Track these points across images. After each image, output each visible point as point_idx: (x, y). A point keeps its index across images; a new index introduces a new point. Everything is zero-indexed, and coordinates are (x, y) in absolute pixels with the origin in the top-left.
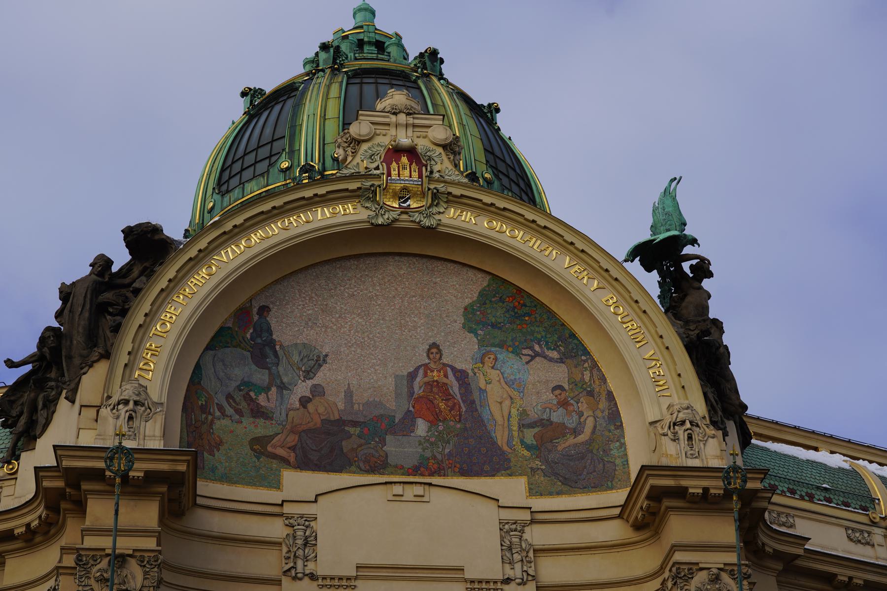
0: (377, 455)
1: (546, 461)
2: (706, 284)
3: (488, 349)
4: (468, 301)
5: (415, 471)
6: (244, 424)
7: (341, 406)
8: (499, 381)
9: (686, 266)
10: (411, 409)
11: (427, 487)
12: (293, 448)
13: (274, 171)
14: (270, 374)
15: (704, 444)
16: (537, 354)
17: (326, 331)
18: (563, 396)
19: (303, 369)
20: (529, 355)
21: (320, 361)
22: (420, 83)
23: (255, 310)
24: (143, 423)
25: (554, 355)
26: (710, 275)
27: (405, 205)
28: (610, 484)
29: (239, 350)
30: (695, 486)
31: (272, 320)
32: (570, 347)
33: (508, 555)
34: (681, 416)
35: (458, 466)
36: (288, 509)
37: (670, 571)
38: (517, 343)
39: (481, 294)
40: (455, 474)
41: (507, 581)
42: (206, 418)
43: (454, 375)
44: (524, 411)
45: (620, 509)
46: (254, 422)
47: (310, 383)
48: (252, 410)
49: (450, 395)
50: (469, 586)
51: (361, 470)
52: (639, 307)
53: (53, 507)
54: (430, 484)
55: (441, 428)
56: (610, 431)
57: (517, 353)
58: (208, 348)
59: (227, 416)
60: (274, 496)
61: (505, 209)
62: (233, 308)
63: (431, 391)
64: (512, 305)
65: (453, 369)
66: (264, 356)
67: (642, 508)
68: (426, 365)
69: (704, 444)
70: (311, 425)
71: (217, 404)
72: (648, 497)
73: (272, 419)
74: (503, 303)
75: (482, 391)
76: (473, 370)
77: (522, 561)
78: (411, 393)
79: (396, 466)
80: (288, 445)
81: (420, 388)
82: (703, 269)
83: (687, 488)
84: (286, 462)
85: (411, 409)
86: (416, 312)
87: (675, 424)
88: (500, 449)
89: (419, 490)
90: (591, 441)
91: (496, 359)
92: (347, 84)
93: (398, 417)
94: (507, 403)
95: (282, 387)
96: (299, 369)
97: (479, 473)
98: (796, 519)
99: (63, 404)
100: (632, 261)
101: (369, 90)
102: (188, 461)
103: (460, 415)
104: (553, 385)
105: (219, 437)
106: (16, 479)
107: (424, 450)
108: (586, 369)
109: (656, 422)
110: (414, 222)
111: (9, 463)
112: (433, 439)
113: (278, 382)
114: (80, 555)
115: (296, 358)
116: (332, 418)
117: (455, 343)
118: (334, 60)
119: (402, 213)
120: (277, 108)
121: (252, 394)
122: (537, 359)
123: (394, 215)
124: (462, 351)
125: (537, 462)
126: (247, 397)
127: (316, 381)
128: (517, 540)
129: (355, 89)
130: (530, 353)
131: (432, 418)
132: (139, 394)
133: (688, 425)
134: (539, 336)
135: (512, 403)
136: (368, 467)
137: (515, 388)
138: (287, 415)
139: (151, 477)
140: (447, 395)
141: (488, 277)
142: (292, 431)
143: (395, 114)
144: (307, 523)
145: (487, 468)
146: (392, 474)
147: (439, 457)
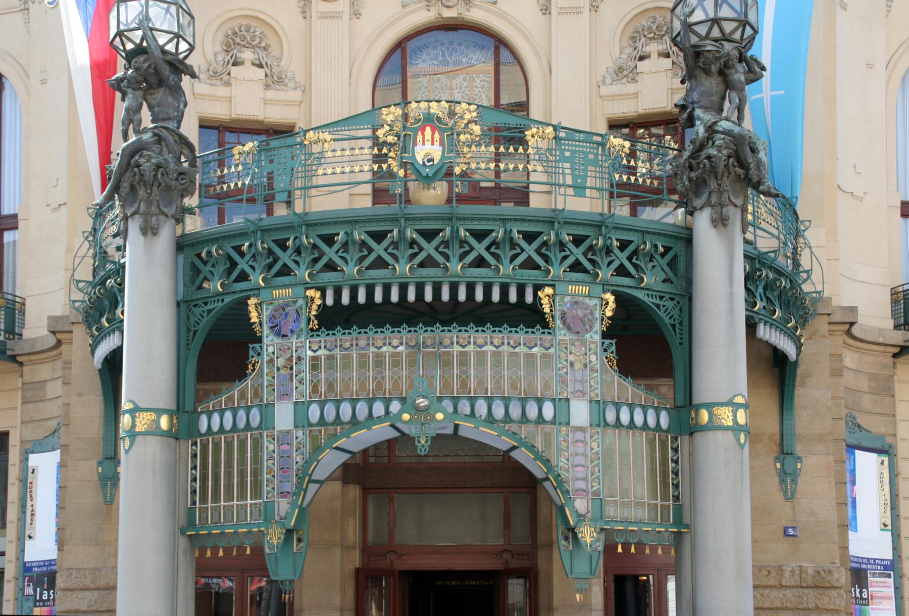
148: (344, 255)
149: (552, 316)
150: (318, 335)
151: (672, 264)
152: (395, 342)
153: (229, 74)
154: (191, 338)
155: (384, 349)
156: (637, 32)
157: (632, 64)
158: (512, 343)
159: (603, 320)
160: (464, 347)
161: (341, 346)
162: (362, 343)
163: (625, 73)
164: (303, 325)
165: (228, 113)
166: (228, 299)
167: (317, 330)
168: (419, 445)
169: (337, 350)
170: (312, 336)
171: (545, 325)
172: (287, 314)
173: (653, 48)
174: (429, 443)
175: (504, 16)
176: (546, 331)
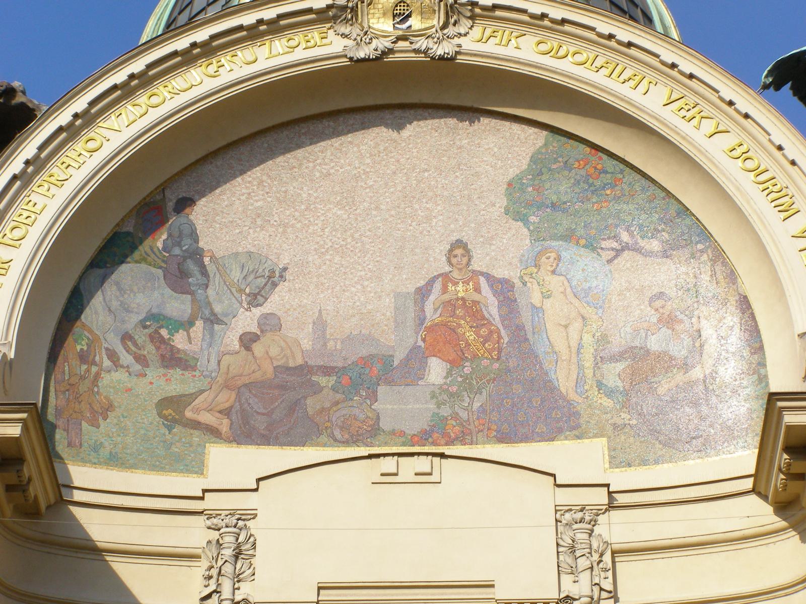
4: (512, 172)
6: (149, 378)
7: (306, 344)
8: (564, 293)
11: (436, 460)
12: (226, 412)
14: (194, 301)
16: (625, 247)
17: (284, 232)
19: (247, 291)
20: (613, 249)
21: (274, 278)
23: (171, 205)
25: (655, 245)
29: (143, 266)
33: (570, 560)
36: (212, 502)
39: (534, 159)
40: (488, 440)
42: (88, 371)
45: (752, 479)
46: (165, 375)
47: (257, 312)
48: (163, 357)
49: (484, 318)
51: (336, 440)
52: (784, 155)
54: (442, 456)
55: (467, 370)
57: (592, 246)
59: (122, 366)
60: (191, 485)
61: (564, 21)
62: (135, 199)
63: (453, 315)
65: (488, 277)
66: (184, 274)
68: (446, 277)
70: (258, 375)
71: (107, 349)
73: (194, 368)
75: (537, 310)
76: (521, 277)
77: (592, 568)
78: (421, 320)
79: (393, 433)
80: (218, 408)
81: (436, 310)
84: (214, 433)
85: (420, 343)
86: (430, 194)
88: (564, 398)
89: (423, 464)
91: (559, 258)
93: (399, 356)
95: (213, 320)
96: (241, 291)
97: (526, 439)
100: (777, 88)
103: (500, 351)
104: (649, 294)
105: (106, 398)
107: (439, 407)
110: (416, 51)
112: (455, 389)
113: (207, 312)
115: (236, 275)
116: (291, 364)
117: (492, 238)
119: (399, 39)
121: (164, 332)
123: (385, 43)
124: (503, 249)
125: (623, 415)
126: (157, 339)
127: (267, 308)
128: (586, 536)
130: (615, 245)
136: (347, 436)
138: (219, 362)
141: (545, 133)
142: (227, 386)
144: (241, 523)
146: (386, 444)
147: (464, 415)
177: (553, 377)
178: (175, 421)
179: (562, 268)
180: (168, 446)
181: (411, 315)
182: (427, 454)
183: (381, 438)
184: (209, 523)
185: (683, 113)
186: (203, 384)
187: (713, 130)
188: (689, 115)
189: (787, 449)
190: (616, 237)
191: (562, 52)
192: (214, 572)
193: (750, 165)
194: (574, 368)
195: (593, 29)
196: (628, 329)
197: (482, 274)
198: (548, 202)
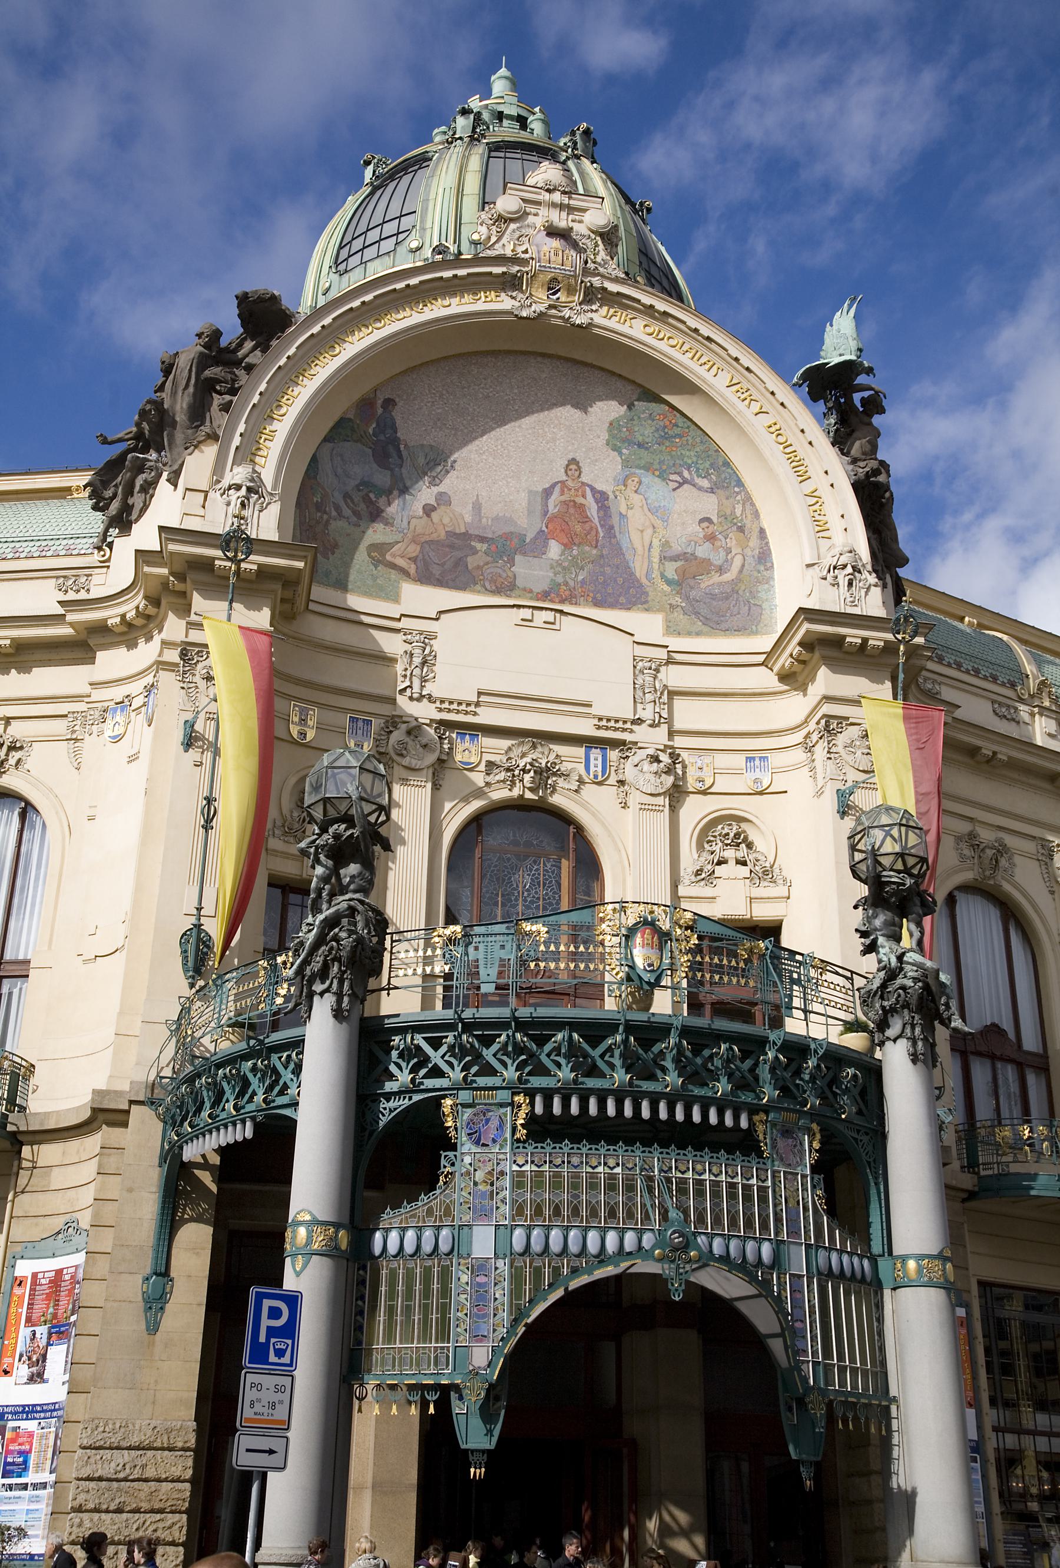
0: (504, 575)
1: (688, 598)
2: (877, 420)
3: (633, 470)
4: (614, 415)
5: (545, 596)
7: (468, 518)
8: (642, 507)
9: (857, 397)
10: (544, 528)
11: (558, 615)
12: (414, 560)
13: (402, 250)
14: (392, 475)
15: (866, 593)
18: (710, 530)
22: (571, 164)
23: (380, 402)
24: (256, 513)
25: (705, 483)
26: (882, 411)
27: (554, 297)
28: (754, 628)
29: (359, 445)
30: (853, 635)
31: (398, 415)
32: (723, 476)
34: (843, 560)
35: (591, 595)
36: (405, 623)
37: (818, 723)
38: (664, 467)
41: (638, 721)
42: (321, 517)
43: (594, 496)
44: (667, 542)
47: (435, 490)
48: (371, 513)
49: (587, 517)
50: (596, 722)
53: (154, 601)
54: (561, 612)
55: (575, 552)
56: (759, 572)
57: (663, 477)
58: (326, 440)
62: (356, 396)
64: (662, 424)
65: (592, 489)
66: (387, 455)
67: (791, 655)
68: (563, 482)
69: (866, 593)
70: (434, 536)
72: (800, 644)
74: (653, 420)
79: (525, 590)
81: (555, 506)
82: (874, 405)
83: (844, 637)
84: (405, 573)
85: (544, 528)
87: (835, 568)
88: (638, 581)
89: (549, 616)
90: (738, 580)
91: (640, 483)
92: (489, 157)
94: (650, 531)
97: (613, 605)
98: (943, 687)
99: (163, 485)
101: (515, 167)
102: (305, 557)
103: (597, 541)
106: (108, 567)
108: (739, 502)
109: (813, 565)
110: (562, 318)
111: (99, 549)
113: (401, 485)
114: (185, 649)
115: (421, 461)
116: (457, 531)
117: (596, 461)
118: (474, 128)
120: (407, 179)
121: (372, 496)
122: (685, 486)
123: (540, 308)
124: (603, 470)
126: (367, 500)
127: (442, 488)
129: (497, 164)
130: (679, 479)
131: (565, 541)
132: (252, 480)
133: (849, 569)
134: (690, 462)
135: (655, 532)
137: (658, 518)
139: (264, 573)
140: (585, 519)
142: (414, 542)
143: (549, 191)
145: (622, 600)
147: (571, 583)
148: (557, 1058)
149: (766, 1144)
150: (524, 1147)
151: (863, 1093)
152: (611, 1162)
153: (304, 832)
154: (366, 1138)
155: (600, 1169)
156: (715, 837)
157: (709, 867)
158: (730, 1173)
159: (810, 1152)
160: (683, 1173)
161: (551, 1162)
162: (575, 1160)
163: (703, 875)
164: (508, 1135)
165: (298, 873)
166: (416, 1098)
167: (524, 1142)
168: (673, 1289)
169: (546, 1167)
170: (518, 1147)
171: (760, 1154)
172: (488, 1121)
173: (730, 853)
174: (683, 1287)
175: (584, 805)
176: (761, 1160)
177: (631, 565)
178: (379, 561)
179: (642, 489)
180: (375, 578)
181: (539, 508)
182: (551, 610)
183: (517, 592)
184: (404, 638)
185: (739, 394)
186: (399, 537)
187: (757, 410)
188: (743, 397)
189: (800, 644)
190: (680, 474)
191: (661, 336)
192: (408, 673)
193: (781, 439)
194: (646, 561)
195: (684, 323)
196: (683, 539)
197: (588, 486)
198: (636, 441)
